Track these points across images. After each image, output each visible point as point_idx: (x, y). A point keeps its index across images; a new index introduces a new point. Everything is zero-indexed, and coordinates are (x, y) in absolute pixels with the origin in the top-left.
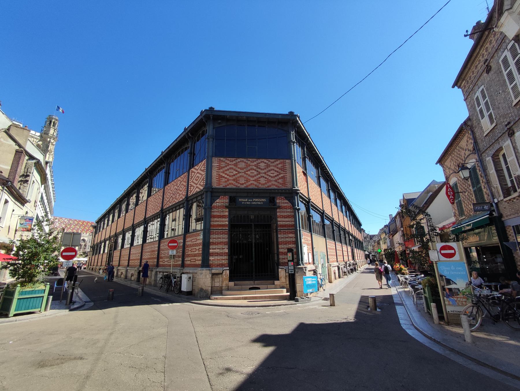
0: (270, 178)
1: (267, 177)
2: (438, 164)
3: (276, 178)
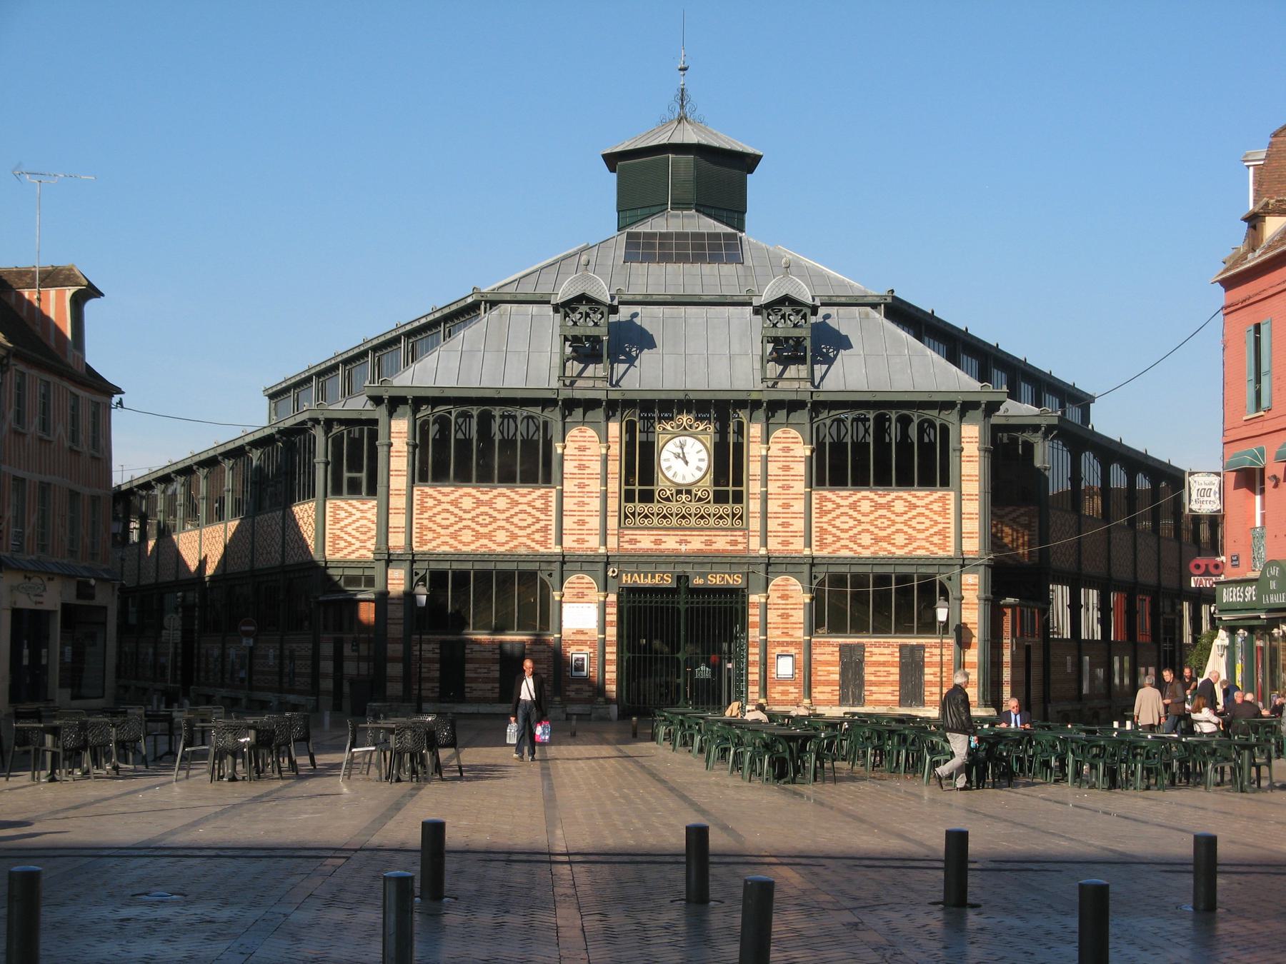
0: (851, 512)
1: (855, 514)
3: (838, 512)
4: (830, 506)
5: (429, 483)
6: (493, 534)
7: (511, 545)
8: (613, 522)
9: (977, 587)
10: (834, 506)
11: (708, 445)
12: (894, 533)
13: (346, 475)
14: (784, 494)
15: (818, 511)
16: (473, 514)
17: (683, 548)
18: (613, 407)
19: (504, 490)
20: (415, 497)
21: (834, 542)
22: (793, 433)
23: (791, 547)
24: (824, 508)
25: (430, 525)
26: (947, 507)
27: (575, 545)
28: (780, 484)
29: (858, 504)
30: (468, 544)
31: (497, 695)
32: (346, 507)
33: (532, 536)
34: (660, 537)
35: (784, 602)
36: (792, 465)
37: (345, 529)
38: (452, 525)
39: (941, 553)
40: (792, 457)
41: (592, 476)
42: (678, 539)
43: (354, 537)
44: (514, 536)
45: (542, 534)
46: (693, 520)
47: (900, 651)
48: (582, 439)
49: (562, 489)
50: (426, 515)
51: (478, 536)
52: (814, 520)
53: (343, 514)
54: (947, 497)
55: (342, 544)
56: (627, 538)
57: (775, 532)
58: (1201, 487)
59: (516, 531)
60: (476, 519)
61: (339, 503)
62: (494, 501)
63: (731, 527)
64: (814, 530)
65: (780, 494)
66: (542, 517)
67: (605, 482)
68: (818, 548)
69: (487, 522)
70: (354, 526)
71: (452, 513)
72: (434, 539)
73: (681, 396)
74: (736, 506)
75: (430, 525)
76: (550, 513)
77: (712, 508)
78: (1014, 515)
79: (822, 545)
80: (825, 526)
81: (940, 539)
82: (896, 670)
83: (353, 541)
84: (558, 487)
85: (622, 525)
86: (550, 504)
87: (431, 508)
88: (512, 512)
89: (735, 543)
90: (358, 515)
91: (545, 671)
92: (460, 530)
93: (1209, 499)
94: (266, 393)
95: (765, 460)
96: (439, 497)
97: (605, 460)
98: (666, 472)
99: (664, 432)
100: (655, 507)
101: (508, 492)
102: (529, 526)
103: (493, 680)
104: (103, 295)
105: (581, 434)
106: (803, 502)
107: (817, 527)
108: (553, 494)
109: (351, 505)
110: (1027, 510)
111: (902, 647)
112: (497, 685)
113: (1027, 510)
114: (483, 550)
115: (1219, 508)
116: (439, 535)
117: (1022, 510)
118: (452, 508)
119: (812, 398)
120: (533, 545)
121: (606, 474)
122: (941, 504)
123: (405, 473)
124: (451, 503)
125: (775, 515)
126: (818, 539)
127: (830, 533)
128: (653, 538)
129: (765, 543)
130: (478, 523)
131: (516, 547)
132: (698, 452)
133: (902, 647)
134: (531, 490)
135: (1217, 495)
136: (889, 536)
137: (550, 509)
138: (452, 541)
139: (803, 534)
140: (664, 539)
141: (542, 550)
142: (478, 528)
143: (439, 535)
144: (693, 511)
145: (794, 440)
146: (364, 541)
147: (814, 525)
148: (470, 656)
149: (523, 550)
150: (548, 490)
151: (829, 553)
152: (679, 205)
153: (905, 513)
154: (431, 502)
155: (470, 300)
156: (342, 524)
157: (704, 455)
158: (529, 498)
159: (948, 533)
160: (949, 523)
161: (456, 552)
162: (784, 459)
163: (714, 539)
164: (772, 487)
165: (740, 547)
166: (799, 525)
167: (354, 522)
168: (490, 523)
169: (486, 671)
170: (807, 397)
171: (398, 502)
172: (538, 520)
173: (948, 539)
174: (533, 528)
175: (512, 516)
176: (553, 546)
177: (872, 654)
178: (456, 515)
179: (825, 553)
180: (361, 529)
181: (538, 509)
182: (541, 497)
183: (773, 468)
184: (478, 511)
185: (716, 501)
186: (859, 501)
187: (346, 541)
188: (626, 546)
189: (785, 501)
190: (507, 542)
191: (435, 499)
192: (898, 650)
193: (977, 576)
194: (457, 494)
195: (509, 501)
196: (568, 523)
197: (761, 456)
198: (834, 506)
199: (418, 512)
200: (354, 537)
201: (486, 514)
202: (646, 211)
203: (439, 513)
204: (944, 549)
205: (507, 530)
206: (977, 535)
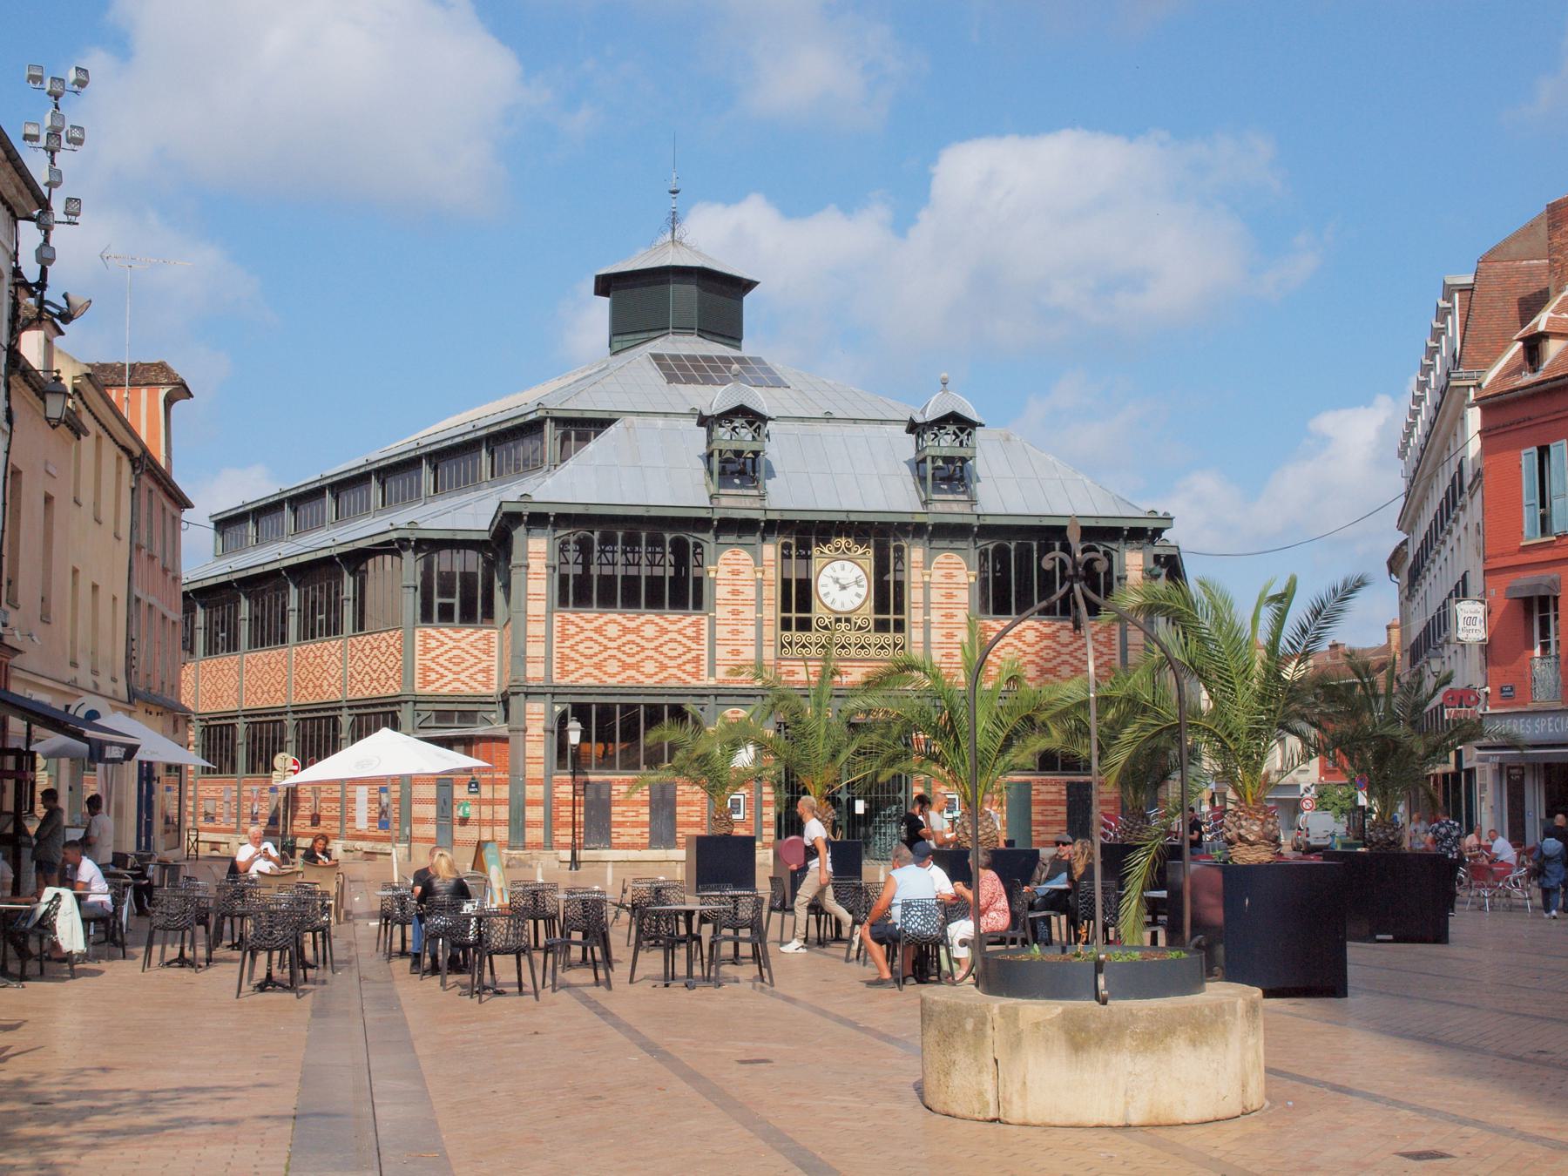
5: (571, 608)
6: (641, 664)
7: (661, 676)
11: (868, 571)
12: (1059, 665)
13: (437, 601)
16: (619, 642)
18: (771, 528)
19: (652, 617)
20: (556, 624)
25: (573, 654)
29: (1023, 634)
30: (613, 676)
31: (647, 841)
32: (438, 635)
33: (683, 667)
37: (437, 660)
38: (596, 654)
43: (446, 668)
44: (663, 667)
45: (694, 665)
46: (853, 650)
47: (1068, 789)
50: (567, 644)
51: (625, 666)
53: (434, 644)
55: (433, 676)
56: (784, 669)
58: (1467, 616)
59: (666, 661)
60: (623, 649)
61: (429, 631)
62: (642, 628)
66: (694, 646)
67: (759, 609)
69: (634, 651)
70: (446, 656)
71: (596, 641)
72: (577, 670)
73: (842, 517)
74: (898, 635)
75: (573, 654)
76: (701, 642)
77: (874, 637)
82: (1064, 809)
83: (446, 673)
86: (702, 632)
87: (572, 636)
88: (661, 640)
90: (451, 644)
91: (699, 814)
92: (605, 660)
94: (214, 519)
95: (927, 587)
96: (582, 623)
99: (823, 555)
100: (812, 636)
101: (657, 619)
102: (680, 656)
103: (642, 824)
105: (735, 557)
108: (706, 620)
109: (442, 633)
111: (1070, 785)
112: (647, 830)
114: (629, 683)
116: (582, 666)
118: (596, 637)
120: (684, 676)
121: (762, 600)
123: (544, 597)
124: (596, 630)
130: (624, 653)
131: (666, 678)
133: (1070, 785)
134: (681, 616)
136: (1055, 667)
138: (596, 672)
141: (694, 682)
142: (624, 657)
143: (582, 666)
144: (853, 640)
146: (458, 673)
148: (617, 798)
149: (673, 683)
152: (682, 329)
153: (1071, 643)
154: (572, 630)
155: (532, 417)
156: (433, 654)
158: (680, 625)
161: (601, 684)
164: (935, 616)
167: (446, 652)
168: (638, 653)
169: (634, 814)
170: (973, 520)
171: (536, 629)
172: (690, 650)
174: (684, 658)
175: (661, 645)
176: (705, 677)
177: (1039, 792)
178: (600, 644)
180: (454, 660)
181: (689, 638)
182: (693, 624)
183: (935, 596)
184: (624, 639)
185: (876, 631)
186: (1024, 630)
187: (437, 672)
189: (948, 631)
190: (656, 674)
191: (577, 626)
192: (1064, 788)
194: (601, 621)
195: (658, 629)
196: (721, 652)
197: (924, 582)
199: (559, 640)
200: (446, 668)
201: (633, 642)
202: (645, 335)
203: (582, 642)
205: (656, 660)
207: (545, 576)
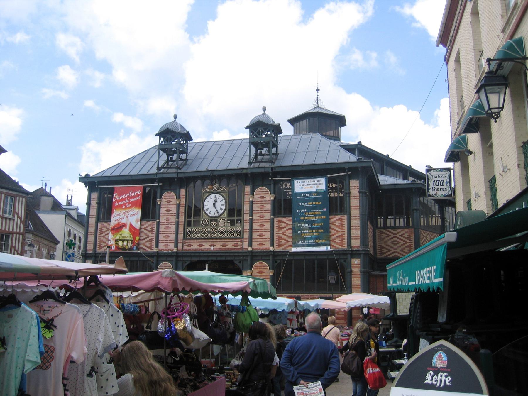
2: (248, 130)
4: (283, 225)
8: (181, 236)
9: (360, 266)
10: (286, 225)
14: (261, 220)
15: (277, 228)
17: (212, 248)
20: (99, 227)
21: (285, 243)
22: (266, 189)
23: (264, 246)
24: (280, 226)
26: (343, 223)
27: (164, 248)
28: (259, 215)
34: (201, 243)
35: (260, 275)
36: (265, 205)
39: (341, 248)
40: (264, 201)
41: (172, 215)
42: (210, 244)
45: (150, 243)
48: (168, 197)
49: (159, 221)
50: (102, 235)
52: (275, 232)
54: (343, 218)
56: (187, 244)
57: (256, 239)
58: (436, 179)
63: (235, 237)
64: (275, 237)
65: (259, 220)
66: (150, 235)
68: (277, 247)
76: (153, 233)
78: (402, 233)
79: (279, 245)
80: (281, 235)
81: (339, 240)
84: (157, 220)
85: (186, 238)
86: (154, 228)
89: (236, 245)
93: (442, 187)
95: (252, 203)
97: (178, 206)
98: (206, 211)
99: (206, 192)
104: (7, 151)
105: (169, 195)
106: (270, 223)
107: (277, 236)
108: (155, 224)
110: (408, 230)
113: (408, 230)
115: (450, 193)
117: (406, 230)
119: (272, 170)
122: (340, 222)
125: (256, 231)
126: (277, 242)
127: (283, 239)
128: (198, 244)
129: (251, 245)
132: (221, 201)
135: (448, 184)
137: (153, 231)
139: (269, 240)
140: (204, 244)
141: (149, 250)
145: (265, 193)
147: (275, 235)
150: (153, 222)
151: (283, 249)
157: (224, 202)
158: (145, 226)
159: (344, 237)
160: (344, 232)
162: (261, 202)
163: (227, 243)
164: (255, 217)
165: (239, 247)
166: (268, 235)
170: (270, 170)
173: (344, 240)
179: (280, 249)
181: (149, 231)
183: (256, 207)
188: (186, 248)
189: (261, 223)
193: (359, 259)
196: (161, 237)
197: (250, 201)
198: (286, 225)
199: (99, 234)
204: (342, 246)
206: (359, 238)
207: (96, 208)
